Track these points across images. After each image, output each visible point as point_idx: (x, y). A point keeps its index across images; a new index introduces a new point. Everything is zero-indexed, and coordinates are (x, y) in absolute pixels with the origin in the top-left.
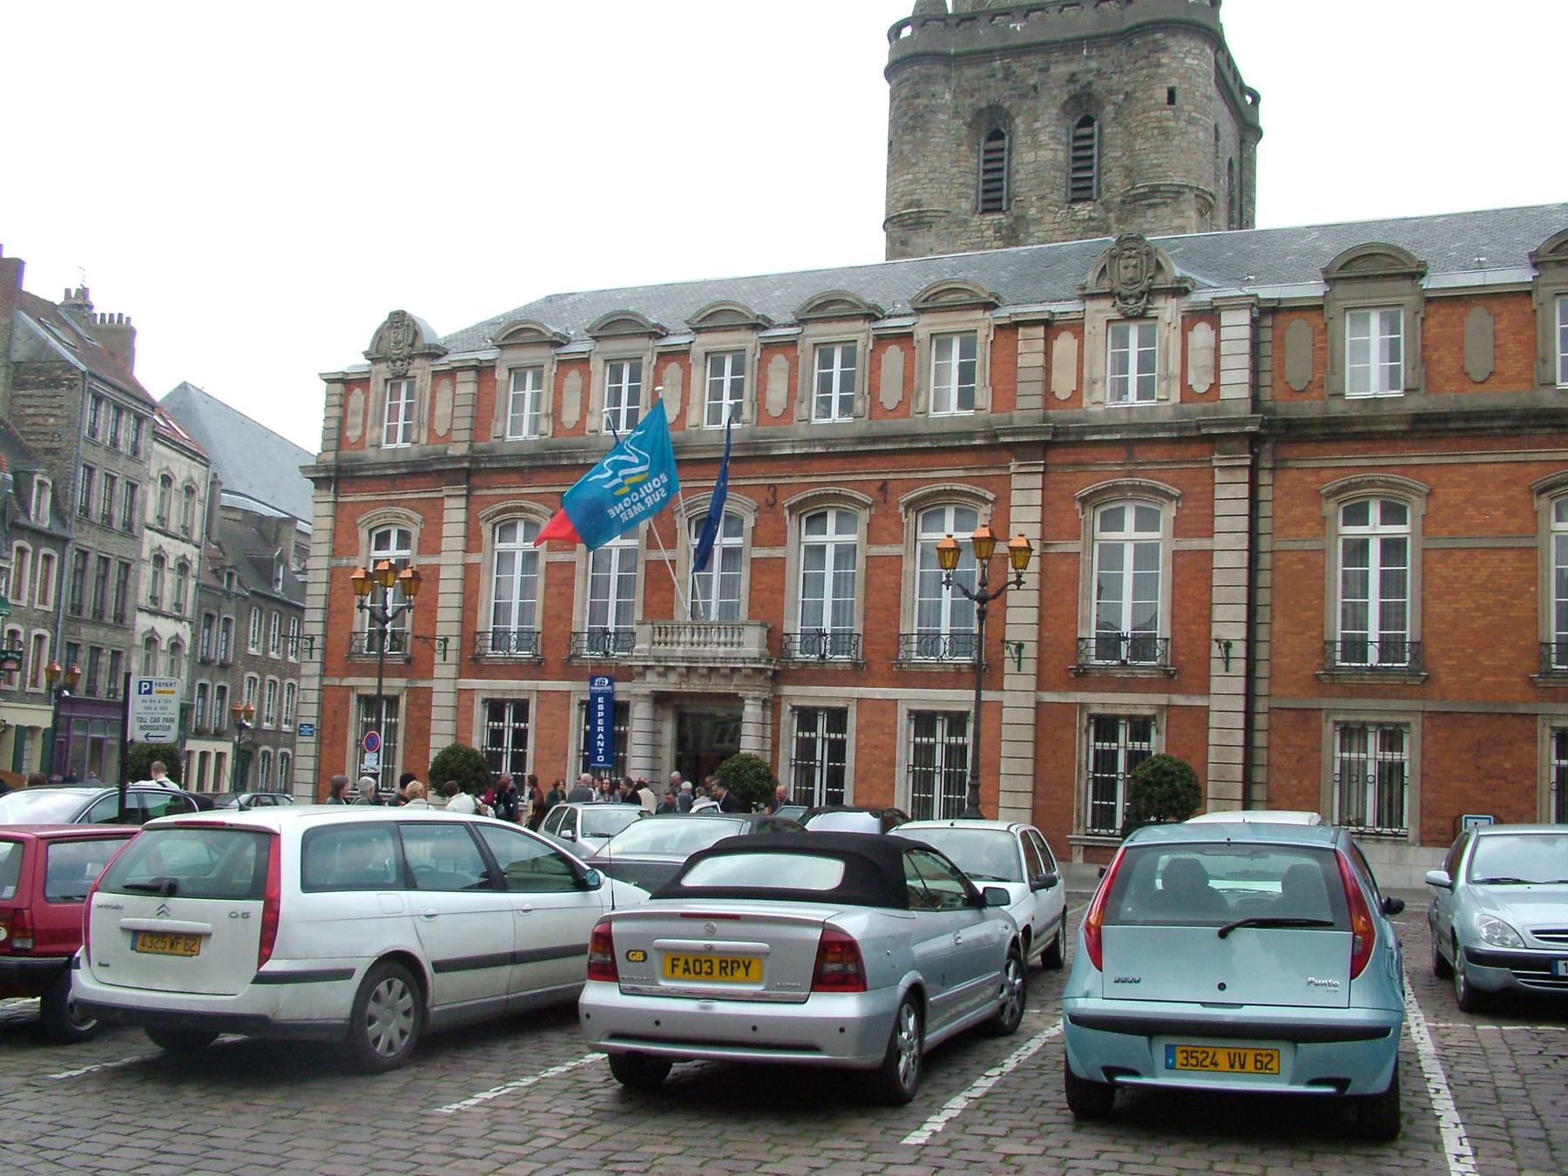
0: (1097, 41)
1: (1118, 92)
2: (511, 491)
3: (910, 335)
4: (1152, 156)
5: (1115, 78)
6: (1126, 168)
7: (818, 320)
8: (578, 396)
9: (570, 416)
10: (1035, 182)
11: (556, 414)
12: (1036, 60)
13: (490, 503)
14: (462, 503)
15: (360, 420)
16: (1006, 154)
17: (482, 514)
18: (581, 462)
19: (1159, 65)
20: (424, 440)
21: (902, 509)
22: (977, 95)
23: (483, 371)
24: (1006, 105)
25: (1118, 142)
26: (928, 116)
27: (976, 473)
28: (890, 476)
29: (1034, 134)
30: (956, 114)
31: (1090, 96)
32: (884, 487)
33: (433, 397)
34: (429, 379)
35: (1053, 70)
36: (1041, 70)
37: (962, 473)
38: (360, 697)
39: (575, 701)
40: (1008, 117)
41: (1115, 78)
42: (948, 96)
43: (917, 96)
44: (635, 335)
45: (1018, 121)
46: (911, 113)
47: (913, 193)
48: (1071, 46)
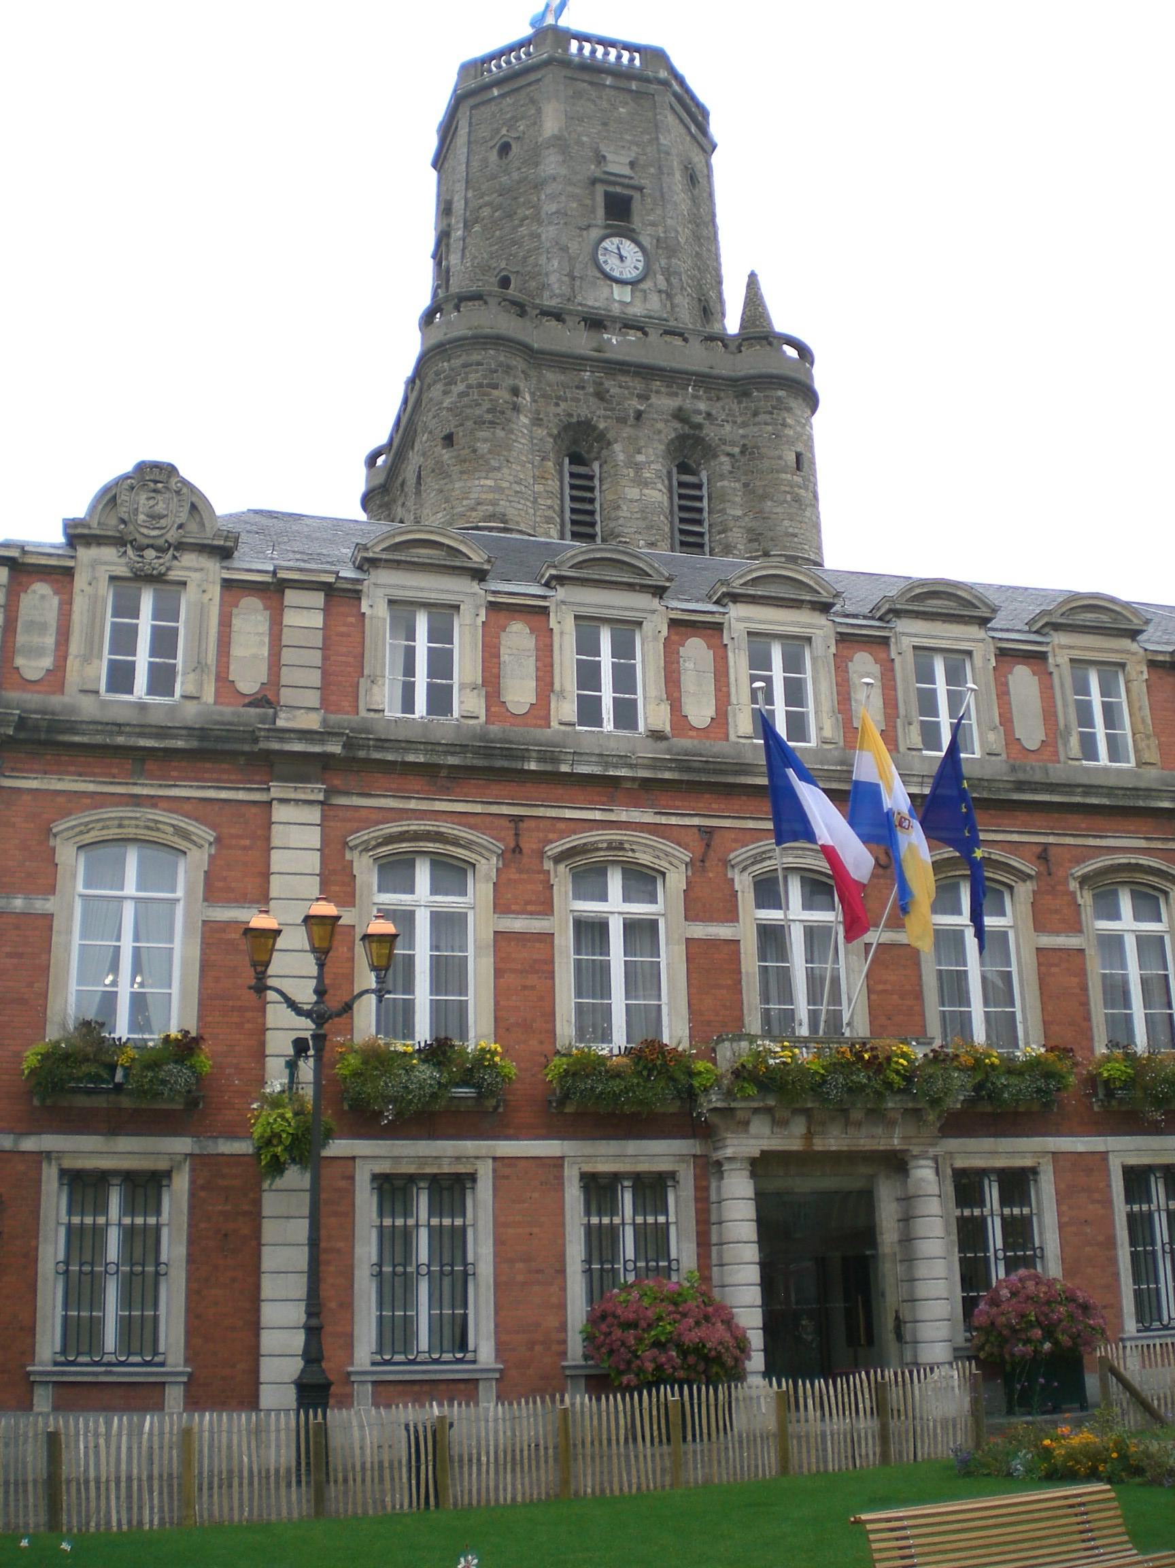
0: (706, 381)
1: (733, 444)
2: (412, 805)
3: (1043, 656)
4: (786, 523)
5: (728, 427)
6: (750, 530)
7: (918, 615)
8: (530, 665)
9: (520, 693)
10: (643, 524)
11: (491, 684)
12: (638, 385)
13: (367, 823)
14: (314, 815)
15: (50, 640)
16: (597, 482)
17: (353, 840)
18: (564, 768)
19: (784, 425)
20: (209, 696)
21: (1073, 885)
22: (563, 405)
23: (340, 596)
24: (602, 426)
25: (738, 499)
26: (509, 413)
27: (1159, 845)
28: (1051, 840)
29: (638, 467)
30: (537, 421)
31: (699, 441)
32: (1043, 855)
33: (225, 623)
34: (215, 591)
35: (654, 400)
36: (639, 396)
37: (1143, 844)
38: (63, 1173)
39: (571, 1175)
40: (603, 440)
41: (728, 427)
42: (528, 398)
43: (495, 386)
44: (631, 587)
45: (617, 447)
46: (487, 405)
47: (494, 503)
48: (674, 378)
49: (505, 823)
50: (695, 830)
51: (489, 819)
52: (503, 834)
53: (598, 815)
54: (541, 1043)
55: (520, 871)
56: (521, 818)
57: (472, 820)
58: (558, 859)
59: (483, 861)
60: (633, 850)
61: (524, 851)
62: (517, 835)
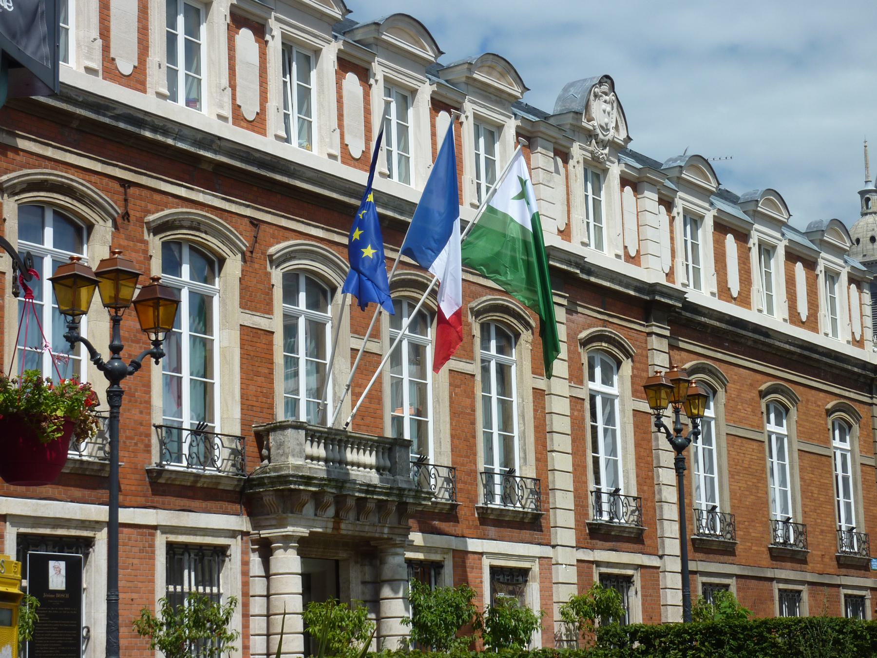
49: (116, 186)
50: (246, 221)
51: (106, 180)
52: (116, 197)
53: (182, 192)
54: (141, 412)
55: (129, 238)
56: (125, 184)
57: (94, 178)
58: (158, 229)
59: (101, 222)
60: (206, 233)
61: (132, 218)
62: (126, 200)
